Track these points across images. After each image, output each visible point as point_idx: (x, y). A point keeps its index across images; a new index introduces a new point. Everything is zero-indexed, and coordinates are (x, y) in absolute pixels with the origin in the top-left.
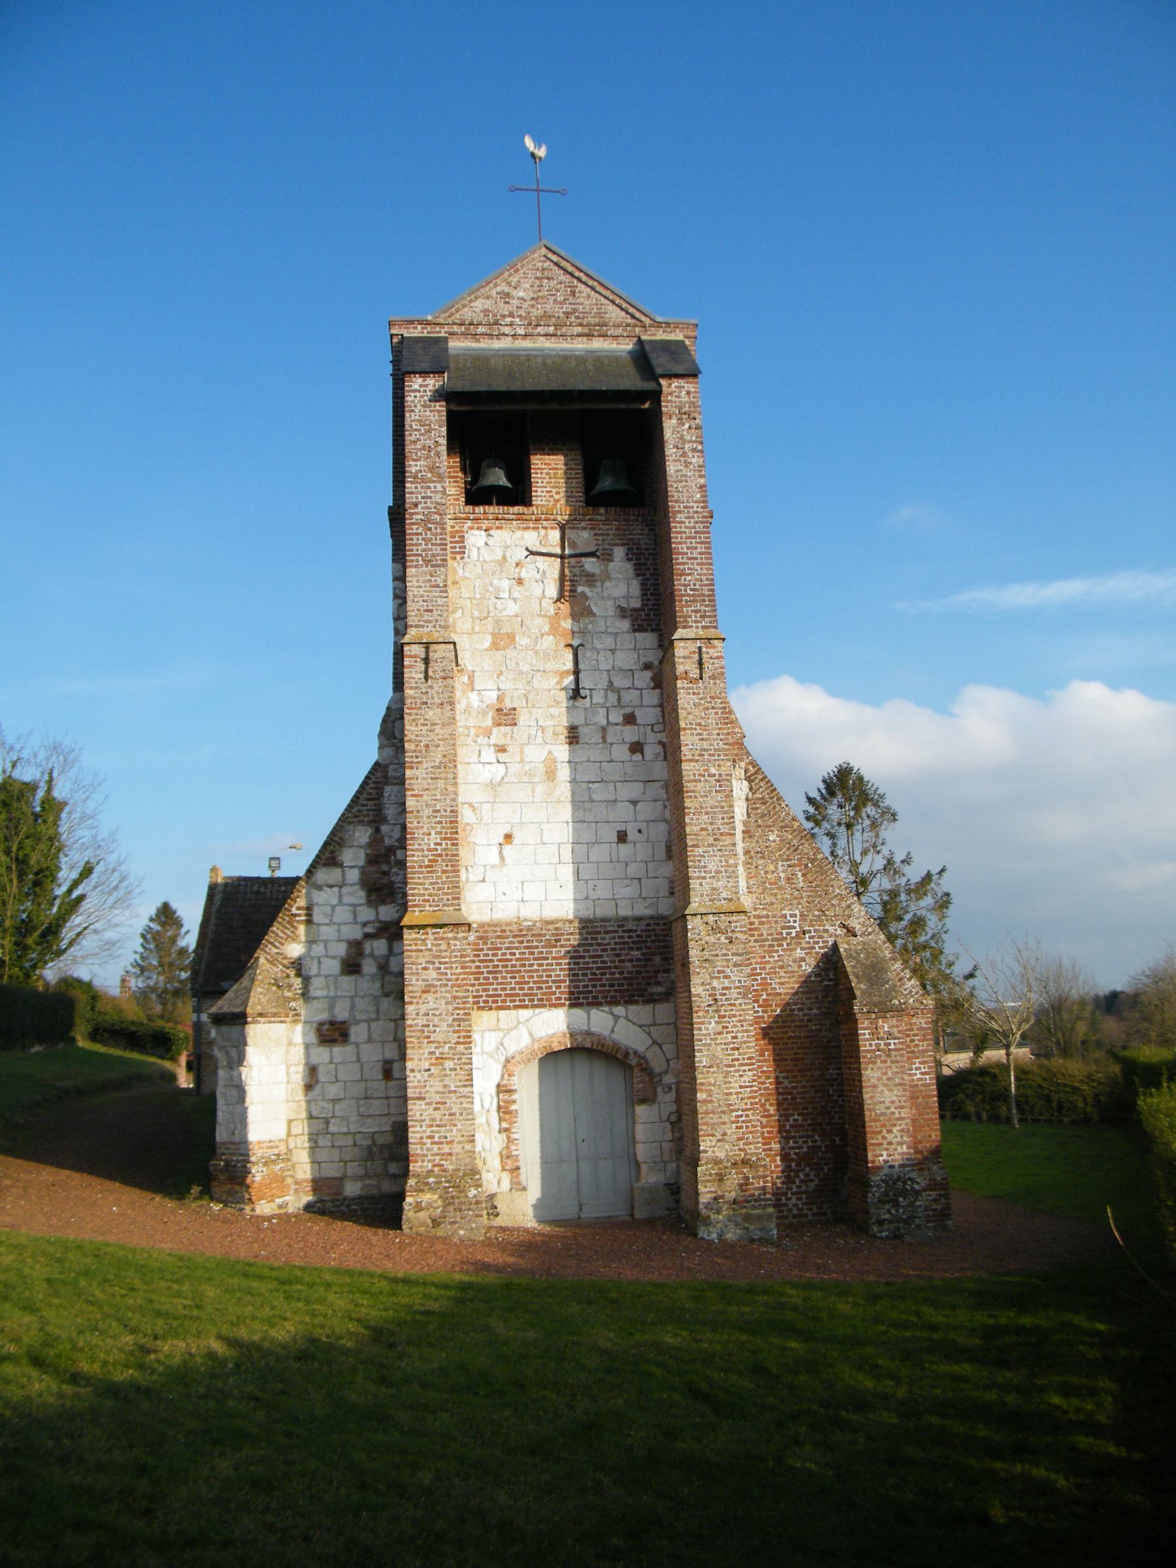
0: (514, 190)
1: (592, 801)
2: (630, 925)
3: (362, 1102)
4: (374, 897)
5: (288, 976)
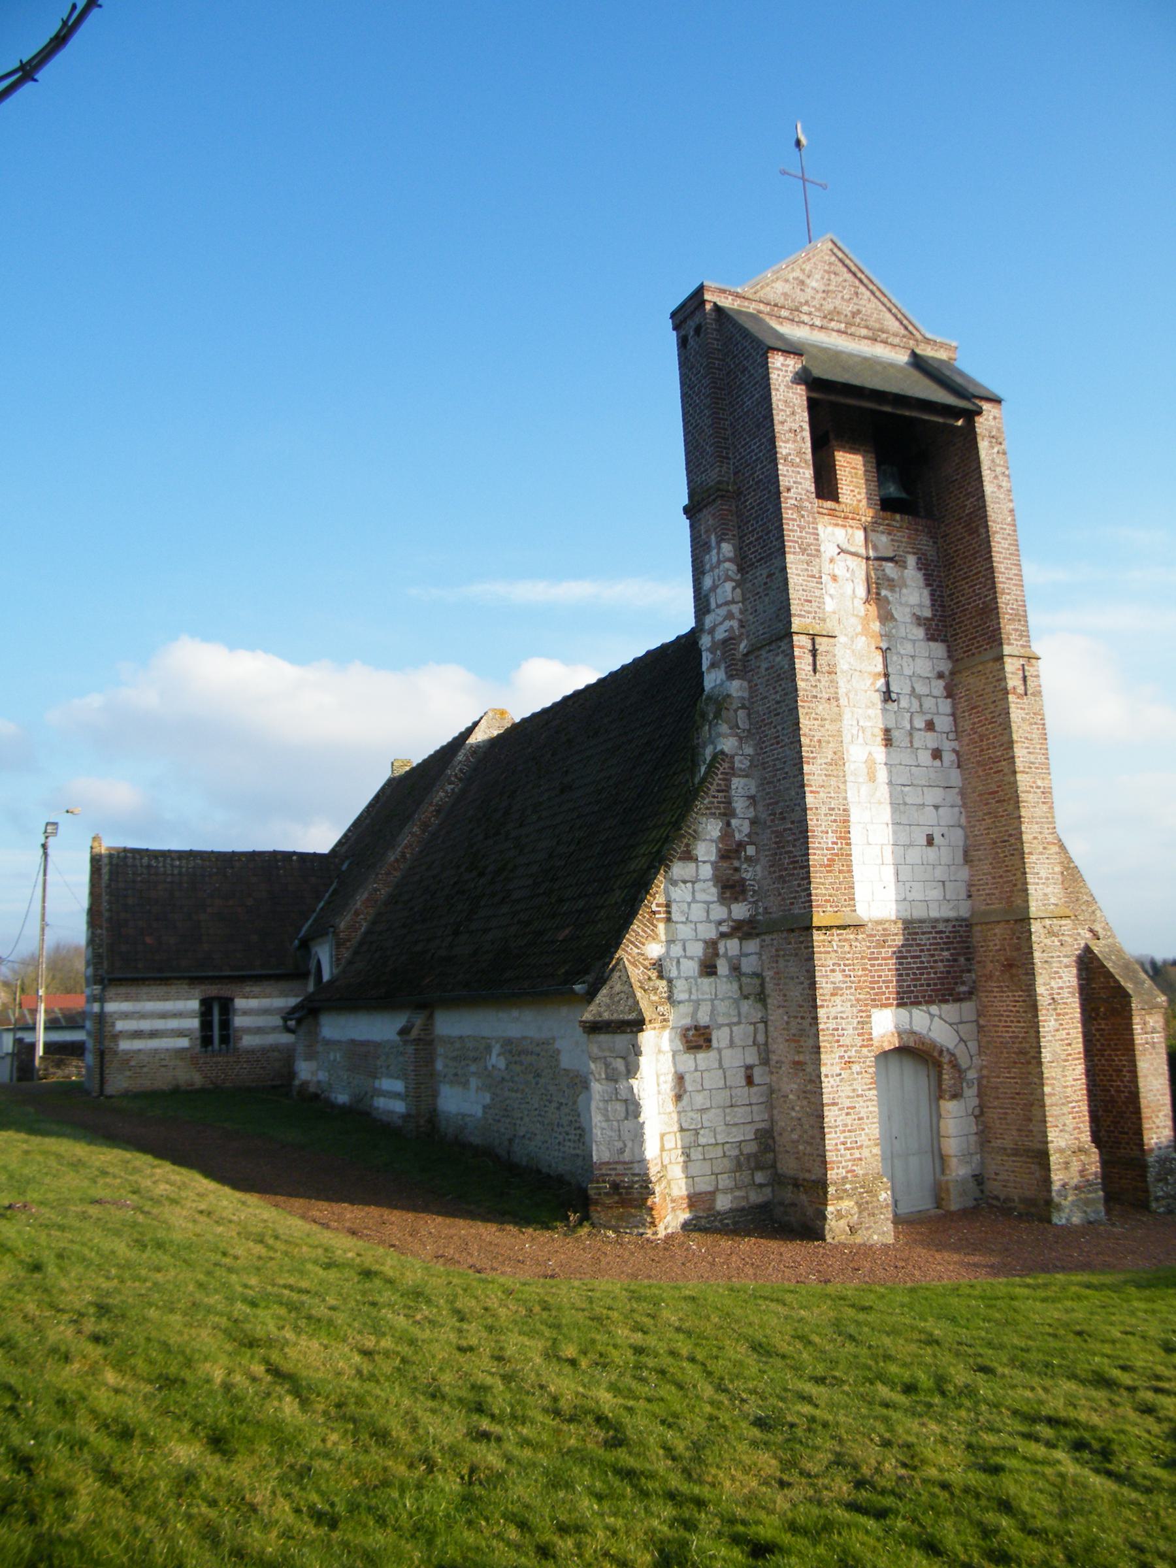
0: (784, 173)
1: (905, 804)
2: (941, 927)
3: (728, 1110)
4: (728, 895)
5: (650, 979)
